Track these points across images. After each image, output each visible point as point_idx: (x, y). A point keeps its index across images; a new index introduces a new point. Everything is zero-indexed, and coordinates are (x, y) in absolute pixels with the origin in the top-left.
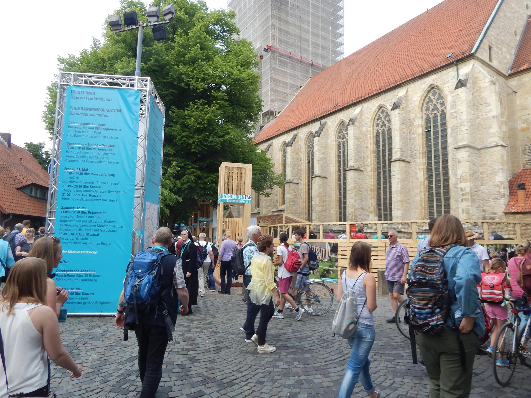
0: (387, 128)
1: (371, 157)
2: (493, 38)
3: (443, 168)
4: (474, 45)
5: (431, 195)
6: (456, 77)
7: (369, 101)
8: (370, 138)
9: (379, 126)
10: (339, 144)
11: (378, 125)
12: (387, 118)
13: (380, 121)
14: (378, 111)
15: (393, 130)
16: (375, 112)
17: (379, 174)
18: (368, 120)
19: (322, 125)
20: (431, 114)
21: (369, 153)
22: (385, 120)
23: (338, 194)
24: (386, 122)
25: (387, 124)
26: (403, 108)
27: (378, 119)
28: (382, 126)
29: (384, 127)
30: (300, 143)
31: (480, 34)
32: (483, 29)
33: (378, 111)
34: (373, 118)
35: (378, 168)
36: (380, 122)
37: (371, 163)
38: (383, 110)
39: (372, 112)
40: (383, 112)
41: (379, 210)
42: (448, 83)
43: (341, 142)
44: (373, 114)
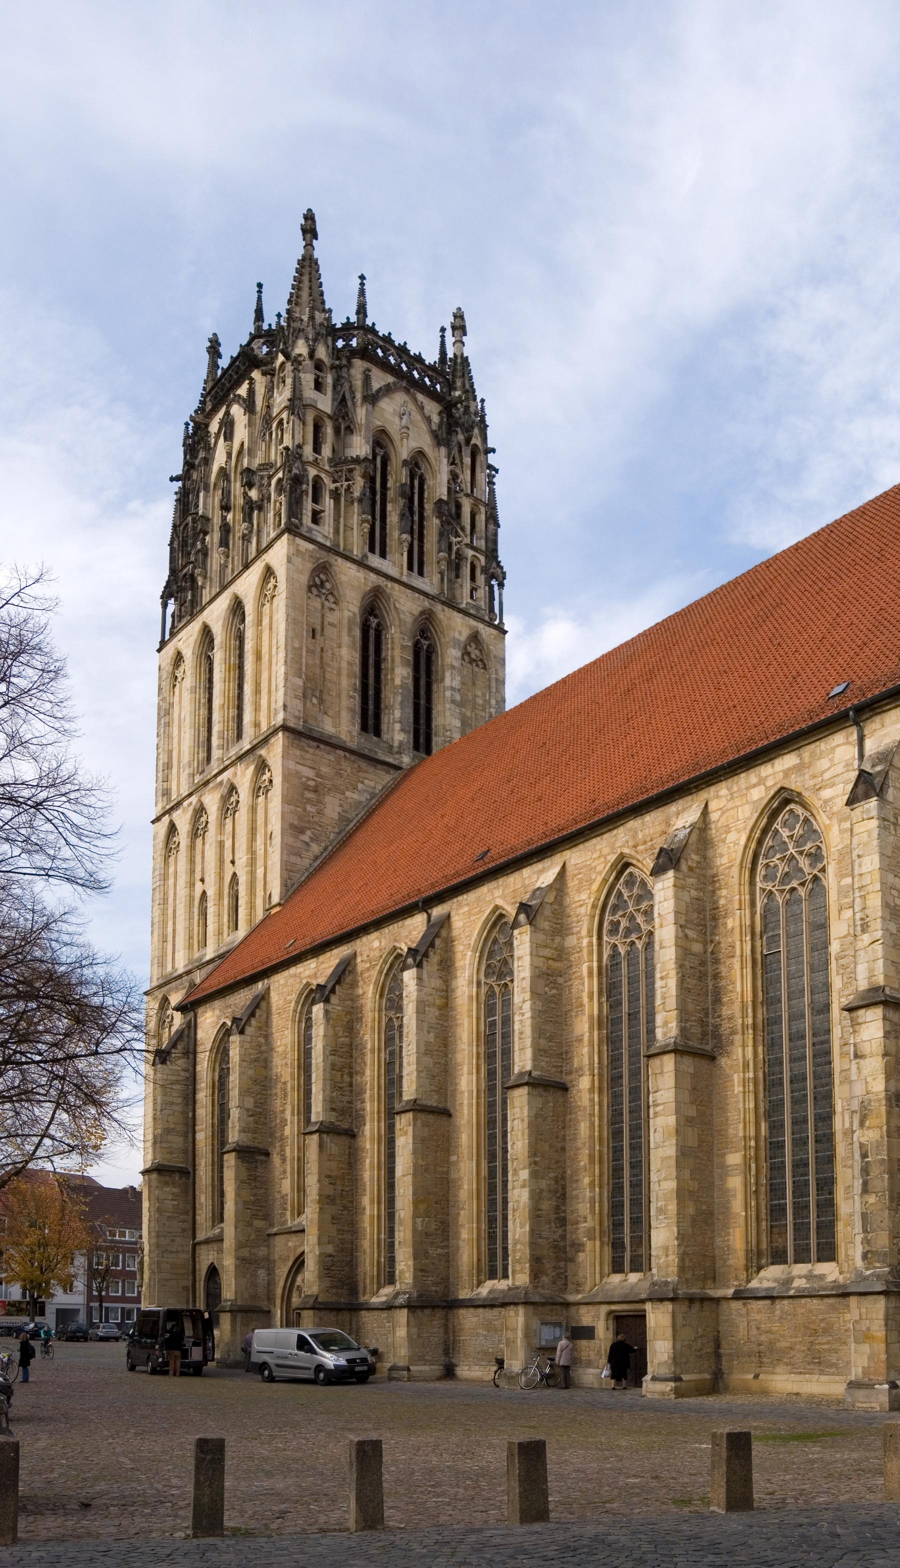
0: (644, 939)
1: (591, 1042)
3: (816, 1076)
5: (777, 1169)
7: (587, 844)
8: (590, 974)
9: (617, 930)
10: (491, 994)
11: (615, 928)
12: (644, 906)
13: (620, 913)
14: (617, 878)
15: (657, 947)
16: (605, 880)
17: (616, 1098)
18: (582, 910)
19: (433, 925)
20: (782, 891)
21: (586, 1027)
22: (639, 910)
23: (484, 1172)
24: (640, 919)
25: (643, 927)
26: (691, 869)
27: (615, 908)
28: (628, 932)
29: (633, 937)
30: (360, 991)
33: (617, 878)
34: (600, 903)
35: (615, 1080)
36: (623, 916)
37: (591, 1058)
38: (631, 874)
39: (595, 887)
40: (630, 883)
41: (618, 1225)
43: (497, 989)
44: (600, 890)
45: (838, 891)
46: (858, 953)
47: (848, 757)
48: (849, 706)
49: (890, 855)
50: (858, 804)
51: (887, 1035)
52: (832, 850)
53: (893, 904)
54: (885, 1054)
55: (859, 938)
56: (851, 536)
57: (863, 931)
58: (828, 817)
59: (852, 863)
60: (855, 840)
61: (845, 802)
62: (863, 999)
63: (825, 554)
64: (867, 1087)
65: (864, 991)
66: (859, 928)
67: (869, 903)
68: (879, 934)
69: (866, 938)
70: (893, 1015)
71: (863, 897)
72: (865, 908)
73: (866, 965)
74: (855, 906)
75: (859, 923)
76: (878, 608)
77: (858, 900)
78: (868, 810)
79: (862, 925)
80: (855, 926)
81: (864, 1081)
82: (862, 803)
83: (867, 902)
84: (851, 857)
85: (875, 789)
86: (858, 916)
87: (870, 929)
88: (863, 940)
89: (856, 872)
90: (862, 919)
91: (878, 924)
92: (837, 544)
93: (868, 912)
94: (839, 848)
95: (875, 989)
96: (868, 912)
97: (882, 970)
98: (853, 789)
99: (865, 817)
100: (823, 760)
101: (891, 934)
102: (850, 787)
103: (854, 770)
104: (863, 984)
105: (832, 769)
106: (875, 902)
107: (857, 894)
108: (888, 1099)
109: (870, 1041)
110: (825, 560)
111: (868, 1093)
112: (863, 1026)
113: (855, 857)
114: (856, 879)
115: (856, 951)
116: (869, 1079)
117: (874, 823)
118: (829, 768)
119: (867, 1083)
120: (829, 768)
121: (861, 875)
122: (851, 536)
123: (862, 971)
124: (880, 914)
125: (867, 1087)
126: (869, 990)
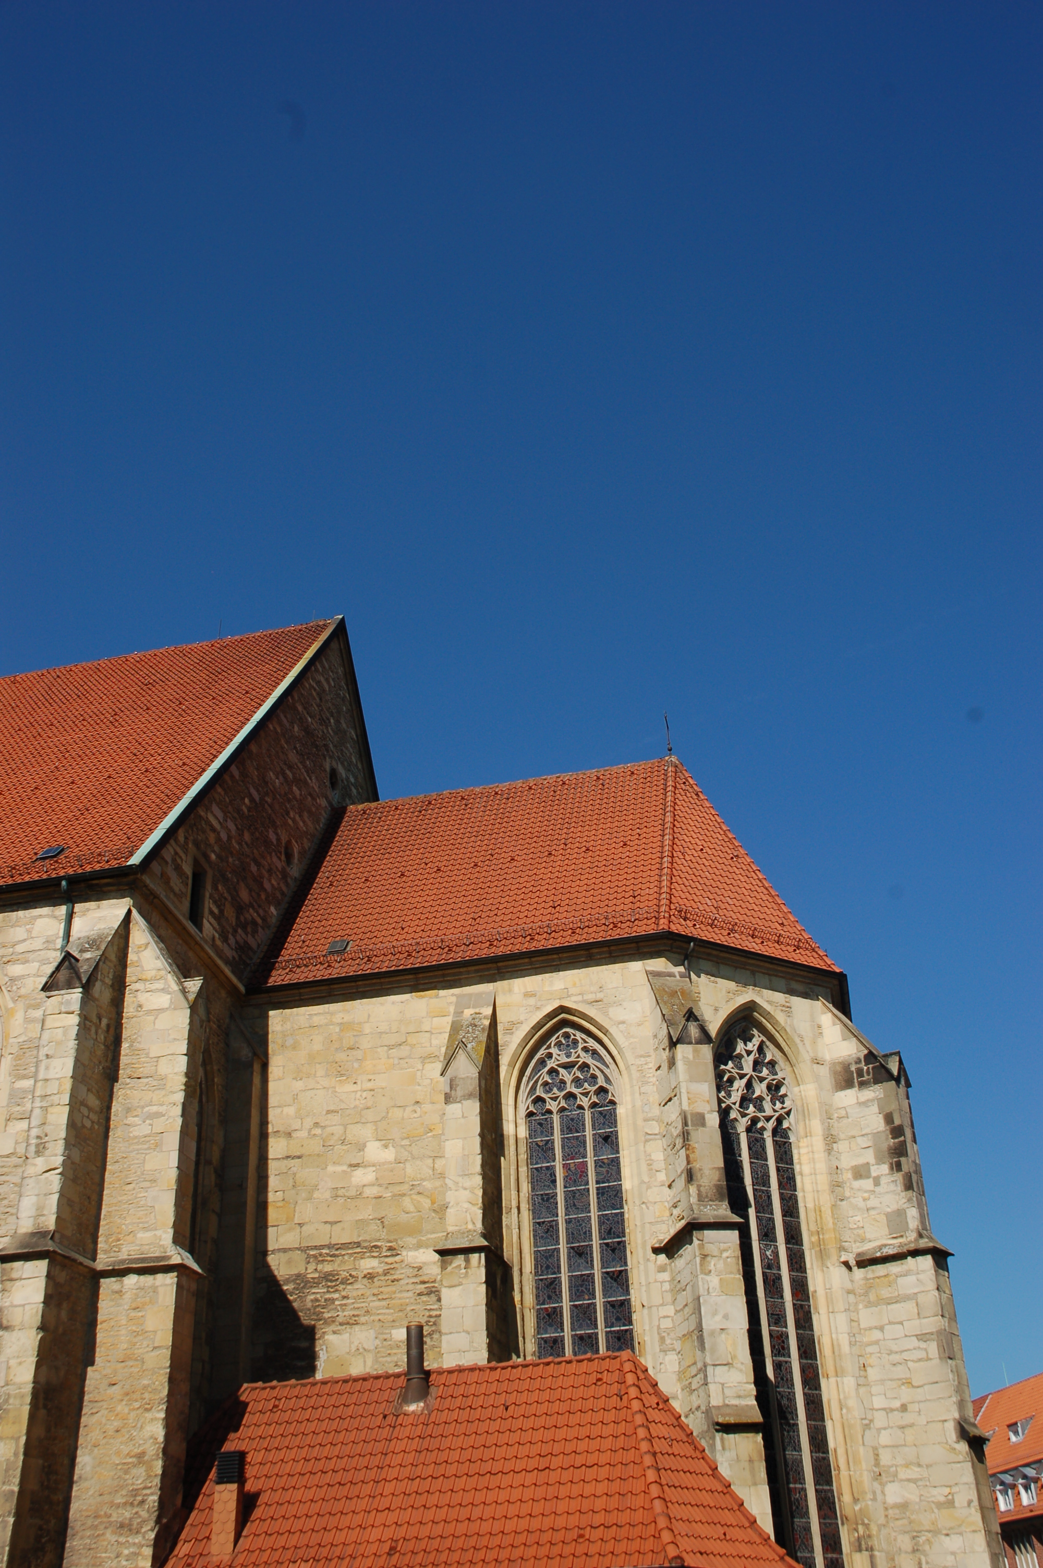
2: (212, 838)
4: (142, 841)
6: (59, 943)
31: (170, 808)
32: (184, 793)
42: (26, 961)
45: (10, 1095)
46: (26, 1181)
47: (50, 933)
48: (62, 873)
49: (86, 1063)
50: (57, 992)
51: (48, 1300)
52: (11, 1040)
53: (79, 1125)
54: (42, 1327)
55: (29, 1161)
56: (81, 689)
57: (38, 1153)
58: (12, 998)
59: (37, 1064)
60: (46, 1035)
61: (41, 986)
62: (23, 1246)
63: (48, 697)
64: (7, 1374)
65: (25, 1234)
66: (33, 1149)
67: (51, 1118)
68: (59, 1160)
69: (40, 1163)
70: (62, 1277)
71: (45, 1109)
72: (44, 1124)
73: (34, 1199)
74: (32, 1119)
75: (34, 1141)
76: (107, 774)
77: (37, 1112)
78: (68, 1002)
79: (37, 1145)
80: (28, 1145)
81: (4, 1366)
82: (62, 992)
83: (49, 1116)
84: (37, 1057)
85: (80, 979)
86: (34, 1132)
87: (47, 1152)
88: (35, 1165)
89: (41, 1076)
90: (38, 1137)
91: (60, 1147)
92: (63, 692)
93: (47, 1129)
94: (21, 1039)
95: (41, 1234)
96: (47, 1129)
97: (54, 1209)
98: (54, 973)
99: (63, 1010)
100: (18, 929)
101: (73, 1163)
102: (50, 969)
103: (56, 950)
104: (26, 1226)
105: (28, 942)
106: (60, 1117)
107: (38, 1104)
108: (35, 1394)
109: (24, 1305)
110: (47, 704)
111: (7, 1384)
112: (18, 1283)
113: (42, 1056)
114: (39, 1084)
115: (23, 1178)
116: (12, 1362)
117: (74, 1020)
118: (25, 940)
119: (8, 1368)
120: (25, 940)
121: (47, 1080)
122: (81, 689)
123: (27, 1206)
124: (63, 1134)
125: (7, 1374)
126: (33, 1234)
